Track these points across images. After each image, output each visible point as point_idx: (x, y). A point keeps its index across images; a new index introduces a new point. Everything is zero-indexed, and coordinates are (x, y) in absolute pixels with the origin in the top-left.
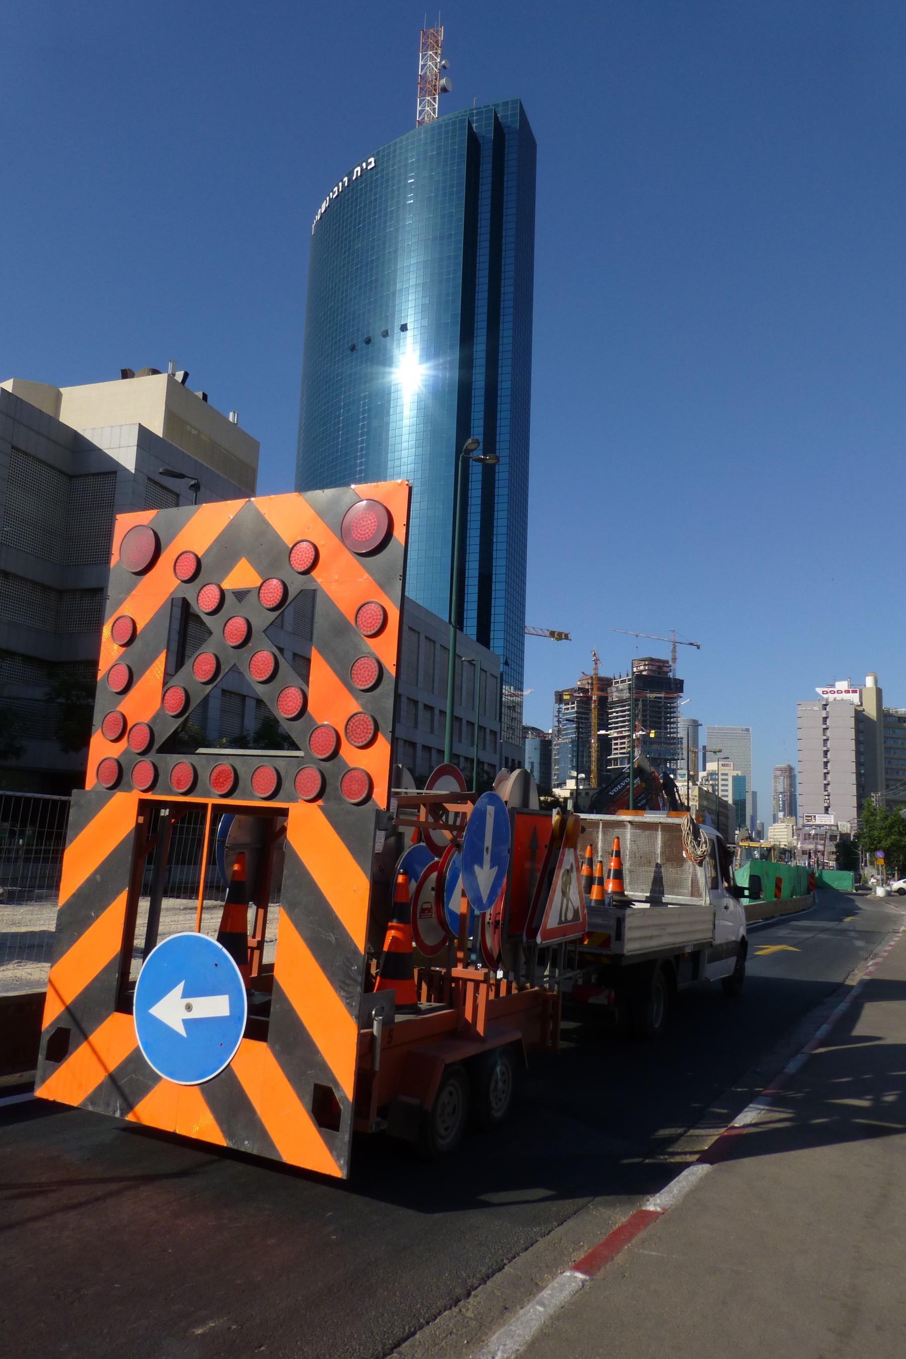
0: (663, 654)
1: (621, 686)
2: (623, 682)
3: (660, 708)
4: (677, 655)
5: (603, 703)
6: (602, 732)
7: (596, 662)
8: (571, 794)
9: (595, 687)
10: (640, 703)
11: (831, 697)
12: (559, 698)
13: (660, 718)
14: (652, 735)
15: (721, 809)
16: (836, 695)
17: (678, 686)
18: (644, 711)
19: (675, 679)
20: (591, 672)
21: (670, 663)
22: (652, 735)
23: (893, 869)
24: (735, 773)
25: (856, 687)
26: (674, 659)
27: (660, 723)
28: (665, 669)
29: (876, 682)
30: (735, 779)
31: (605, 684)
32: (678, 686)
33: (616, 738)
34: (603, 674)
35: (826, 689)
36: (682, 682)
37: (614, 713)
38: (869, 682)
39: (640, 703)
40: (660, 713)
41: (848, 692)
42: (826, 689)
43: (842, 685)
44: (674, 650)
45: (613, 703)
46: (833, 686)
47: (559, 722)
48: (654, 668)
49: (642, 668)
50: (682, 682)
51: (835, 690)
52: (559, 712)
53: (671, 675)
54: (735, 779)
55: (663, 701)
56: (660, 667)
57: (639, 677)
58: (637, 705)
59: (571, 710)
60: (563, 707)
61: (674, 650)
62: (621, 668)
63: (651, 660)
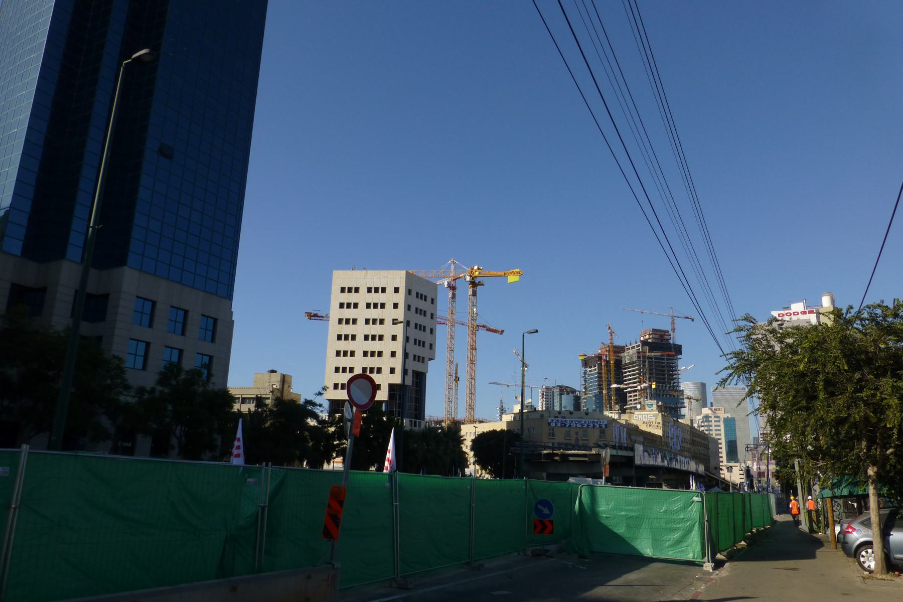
0: (665, 326)
1: (631, 351)
2: (633, 348)
3: (663, 367)
4: (676, 326)
5: (619, 363)
6: (614, 386)
7: (611, 334)
8: (514, 418)
9: (611, 353)
10: (647, 363)
11: (787, 318)
12: (586, 363)
13: (664, 375)
14: (654, 386)
15: (697, 439)
16: (794, 318)
17: (678, 349)
18: (650, 370)
19: (675, 345)
20: (608, 342)
21: (670, 332)
22: (654, 386)
23: (856, 473)
24: (725, 416)
25: (813, 307)
26: (673, 330)
27: (664, 379)
28: (666, 337)
29: (833, 301)
30: (726, 421)
31: (619, 350)
32: (678, 349)
33: (630, 392)
34: (618, 342)
35: (782, 312)
36: (680, 346)
37: (628, 373)
38: (826, 302)
39: (647, 363)
40: (664, 371)
41: (804, 313)
42: (782, 312)
43: (798, 307)
44: (673, 323)
45: (626, 364)
46: (788, 308)
47: (585, 381)
48: (657, 336)
49: (647, 337)
50: (680, 346)
51: (791, 312)
52: (585, 373)
53: (671, 341)
54: (726, 421)
55: (665, 361)
56: (662, 336)
57: (644, 343)
58: (644, 365)
59: (594, 371)
60: (588, 369)
61: (673, 323)
62: (632, 337)
63: (654, 330)
